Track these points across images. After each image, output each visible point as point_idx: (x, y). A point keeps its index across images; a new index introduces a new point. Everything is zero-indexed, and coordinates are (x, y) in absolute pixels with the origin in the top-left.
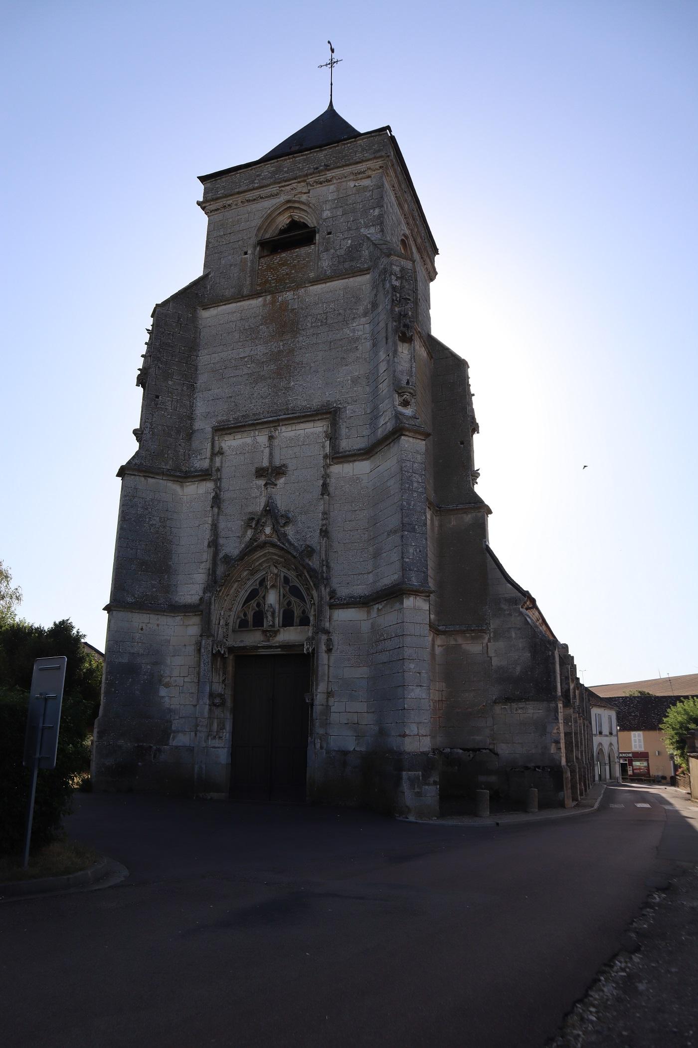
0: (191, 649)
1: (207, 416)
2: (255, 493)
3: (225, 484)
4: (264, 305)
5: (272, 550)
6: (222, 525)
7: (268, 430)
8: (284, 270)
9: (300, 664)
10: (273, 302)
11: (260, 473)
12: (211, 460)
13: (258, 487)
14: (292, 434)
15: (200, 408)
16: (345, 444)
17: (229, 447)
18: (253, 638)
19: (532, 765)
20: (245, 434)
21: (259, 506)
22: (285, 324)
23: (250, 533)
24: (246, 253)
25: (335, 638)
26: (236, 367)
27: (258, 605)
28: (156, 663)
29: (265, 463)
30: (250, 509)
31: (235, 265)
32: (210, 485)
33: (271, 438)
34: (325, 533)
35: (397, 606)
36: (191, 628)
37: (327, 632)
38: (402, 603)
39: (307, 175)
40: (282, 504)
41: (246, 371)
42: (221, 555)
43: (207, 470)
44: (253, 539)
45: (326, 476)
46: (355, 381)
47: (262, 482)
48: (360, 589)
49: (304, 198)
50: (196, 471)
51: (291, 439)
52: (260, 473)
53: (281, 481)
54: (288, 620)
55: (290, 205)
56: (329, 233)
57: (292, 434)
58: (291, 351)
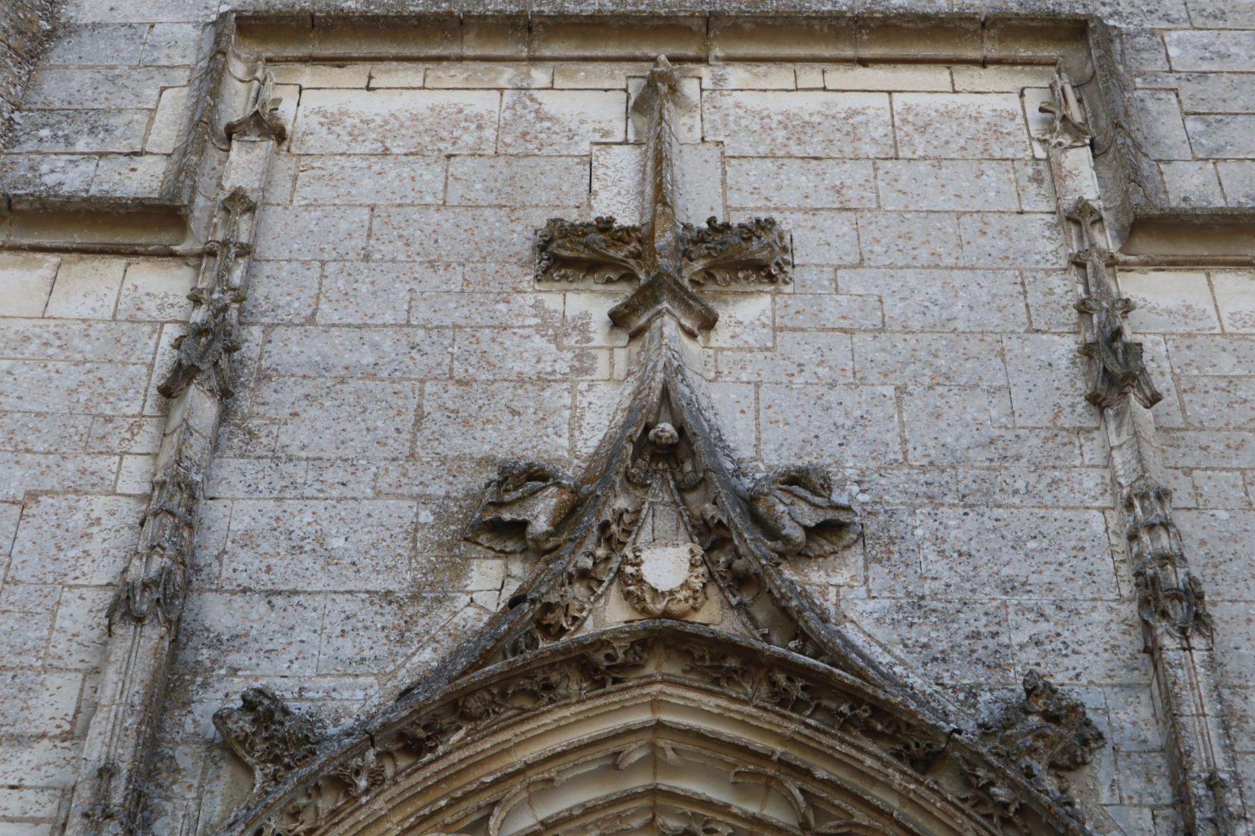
2: (531, 352)
3: (278, 286)
5: (696, 708)
6: (237, 507)
7: (619, 76)
13: (558, 330)
17: (331, 121)
23: (488, 582)
29: (618, 202)
34: (1168, 602)
42: (216, 697)
44: (533, 615)
53: (746, 312)
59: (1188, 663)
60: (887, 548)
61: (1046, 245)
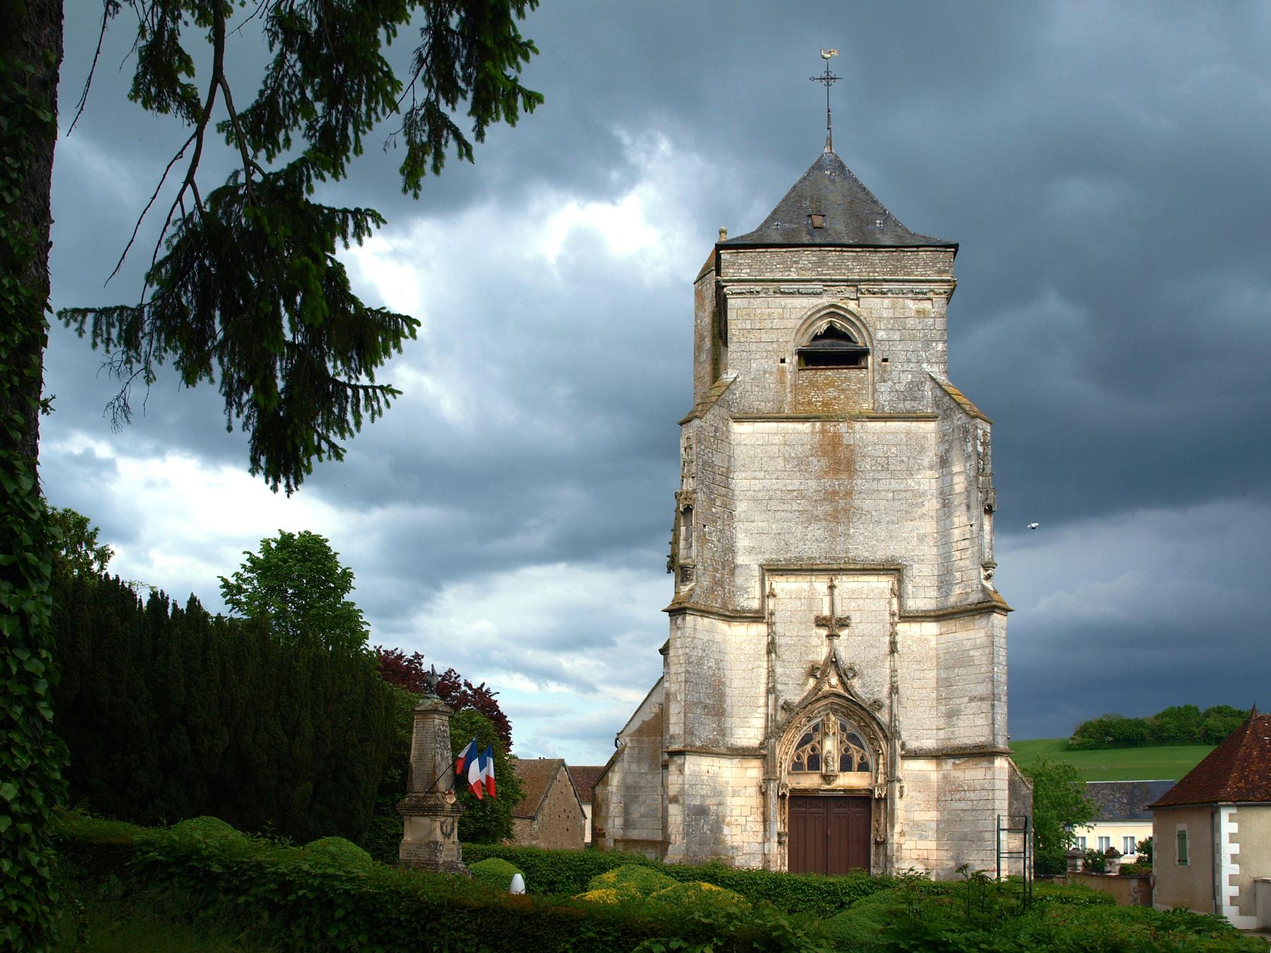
0: (753, 791)
1: (751, 550)
3: (779, 628)
4: (813, 433)
5: (837, 700)
6: (779, 670)
8: (832, 393)
9: (866, 810)
10: (823, 431)
11: (821, 622)
12: (763, 602)
14: (854, 586)
15: (742, 541)
16: (913, 604)
20: (800, 579)
21: (821, 655)
22: (839, 460)
24: (783, 361)
26: (783, 501)
28: (719, 804)
30: (811, 657)
31: (771, 373)
32: (762, 629)
33: (832, 587)
34: (894, 689)
36: (753, 771)
37: (899, 781)
39: (860, 281)
40: (845, 656)
41: (795, 507)
42: (781, 702)
43: (756, 611)
44: (817, 688)
45: (893, 634)
46: (921, 539)
47: (824, 632)
48: (929, 743)
49: (852, 305)
50: (744, 611)
51: (854, 591)
52: (821, 622)
53: (844, 633)
55: (834, 311)
56: (885, 360)
57: (854, 586)
58: (849, 494)
59: (895, 698)
60: (862, 677)
61: (888, 617)
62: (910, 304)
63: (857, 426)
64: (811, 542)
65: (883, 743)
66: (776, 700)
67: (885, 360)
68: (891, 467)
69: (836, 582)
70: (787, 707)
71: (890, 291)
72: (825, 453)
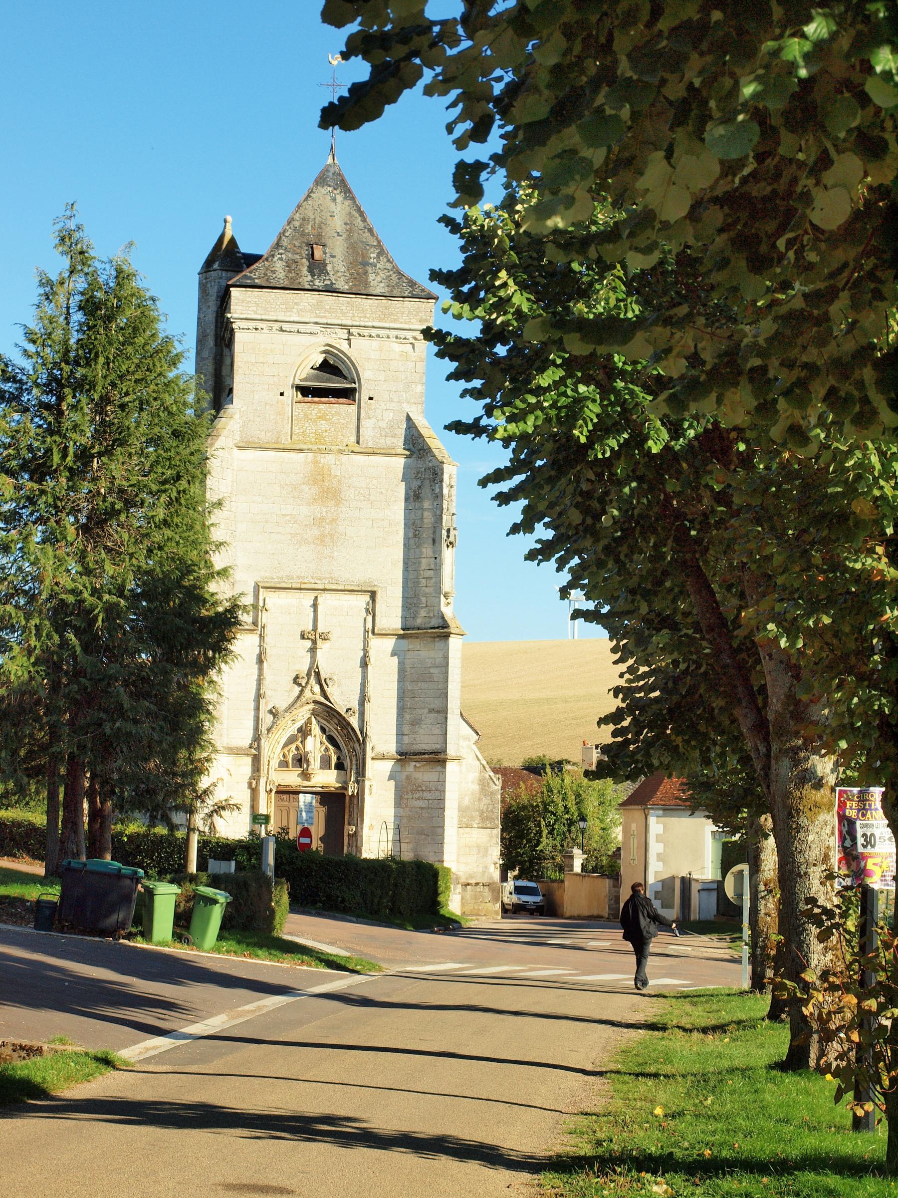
8: (324, 425)
10: (316, 462)
18: (292, 778)
19: (473, 881)
22: (327, 490)
23: (297, 689)
24: (282, 394)
25: (373, 783)
27: (297, 748)
33: (315, 606)
35: (439, 768)
38: (445, 767)
49: (344, 346)
54: (325, 763)
56: (371, 398)
58: (334, 520)
62: (397, 347)
63: (344, 458)
64: (300, 564)
65: (357, 746)
66: (266, 704)
67: (371, 398)
68: (372, 498)
69: (320, 600)
70: (273, 713)
71: (378, 336)
72: (315, 482)
